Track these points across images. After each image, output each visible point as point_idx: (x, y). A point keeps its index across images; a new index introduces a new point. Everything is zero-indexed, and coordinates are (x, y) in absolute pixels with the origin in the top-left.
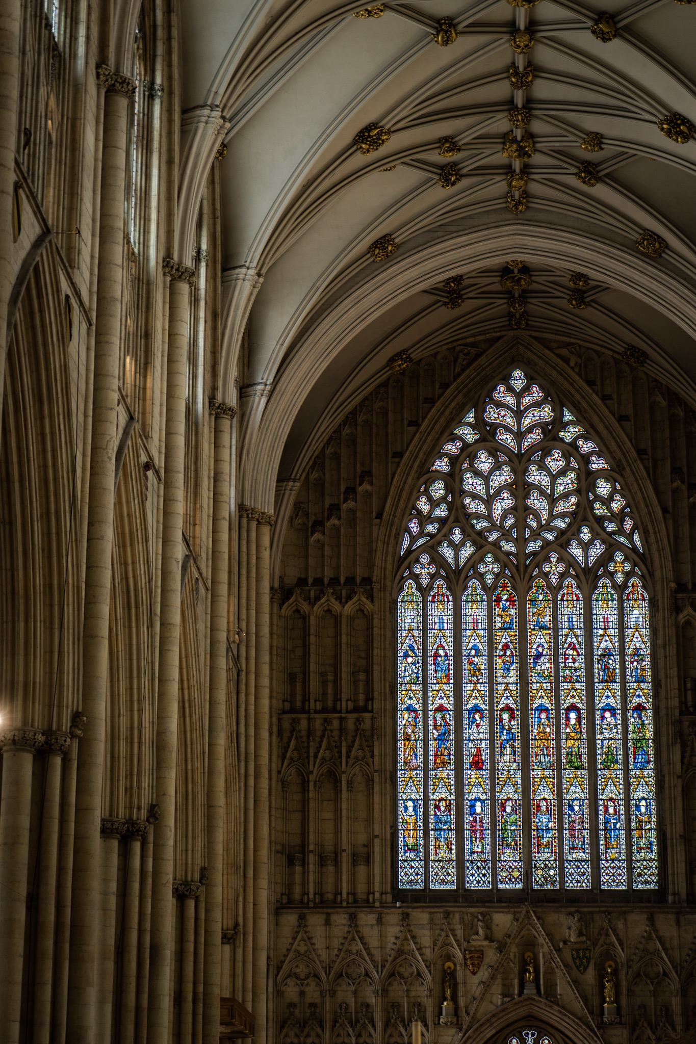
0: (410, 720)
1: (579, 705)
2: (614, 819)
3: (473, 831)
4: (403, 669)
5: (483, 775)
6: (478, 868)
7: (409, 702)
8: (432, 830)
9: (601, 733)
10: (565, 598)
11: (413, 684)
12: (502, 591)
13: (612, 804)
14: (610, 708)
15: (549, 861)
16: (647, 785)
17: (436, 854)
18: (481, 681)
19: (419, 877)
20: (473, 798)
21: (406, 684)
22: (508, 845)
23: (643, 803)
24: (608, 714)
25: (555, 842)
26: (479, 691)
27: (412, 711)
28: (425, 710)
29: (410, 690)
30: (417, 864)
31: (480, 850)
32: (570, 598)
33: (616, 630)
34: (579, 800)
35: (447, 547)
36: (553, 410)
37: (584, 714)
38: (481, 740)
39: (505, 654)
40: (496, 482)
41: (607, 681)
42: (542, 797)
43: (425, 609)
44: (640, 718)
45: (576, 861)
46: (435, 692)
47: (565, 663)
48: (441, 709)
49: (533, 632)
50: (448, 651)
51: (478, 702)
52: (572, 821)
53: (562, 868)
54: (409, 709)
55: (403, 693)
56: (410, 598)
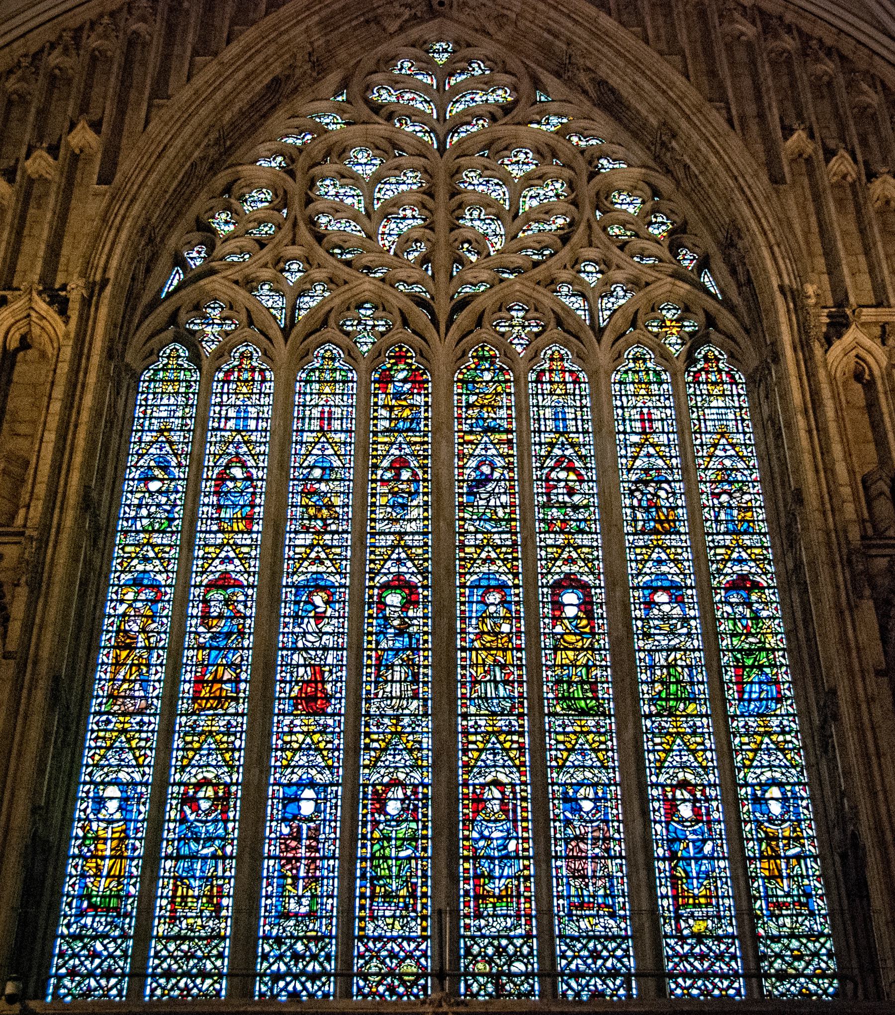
0: (139, 605)
1: (588, 579)
2: (694, 832)
3: (289, 860)
4: (136, 502)
5: (327, 726)
6: (296, 957)
7: (140, 568)
8: (168, 857)
9: (647, 635)
10: (546, 378)
11: (158, 531)
12: (393, 364)
13: (687, 796)
14: (666, 584)
15: (508, 937)
16: (782, 751)
17: (173, 919)
18: (334, 527)
19: (113, 981)
20: (295, 778)
21: (137, 532)
22: (388, 896)
23: (775, 792)
24: (661, 597)
25: (528, 889)
26: (325, 547)
27: (147, 587)
28: (184, 585)
29: (148, 544)
30: (112, 947)
31: (303, 910)
32: (557, 379)
33: (671, 436)
34: (595, 785)
35: (270, 290)
36: (515, 89)
37: (599, 595)
38: (325, 649)
39: (397, 478)
40: (390, 193)
41: (655, 532)
42: (489, 778)
43: (206, 392)
44: (750, 605)
45: (590, 938)
46: (212, 549)
47: (548, 494)
48: (224, 582)
49: (467, 438)
50: (254, 471)
51: (322, 569)
52: (576, 838)
53: (548, 955)
54: (137, 583)
55: (127, 549)
56: (171, 375)
